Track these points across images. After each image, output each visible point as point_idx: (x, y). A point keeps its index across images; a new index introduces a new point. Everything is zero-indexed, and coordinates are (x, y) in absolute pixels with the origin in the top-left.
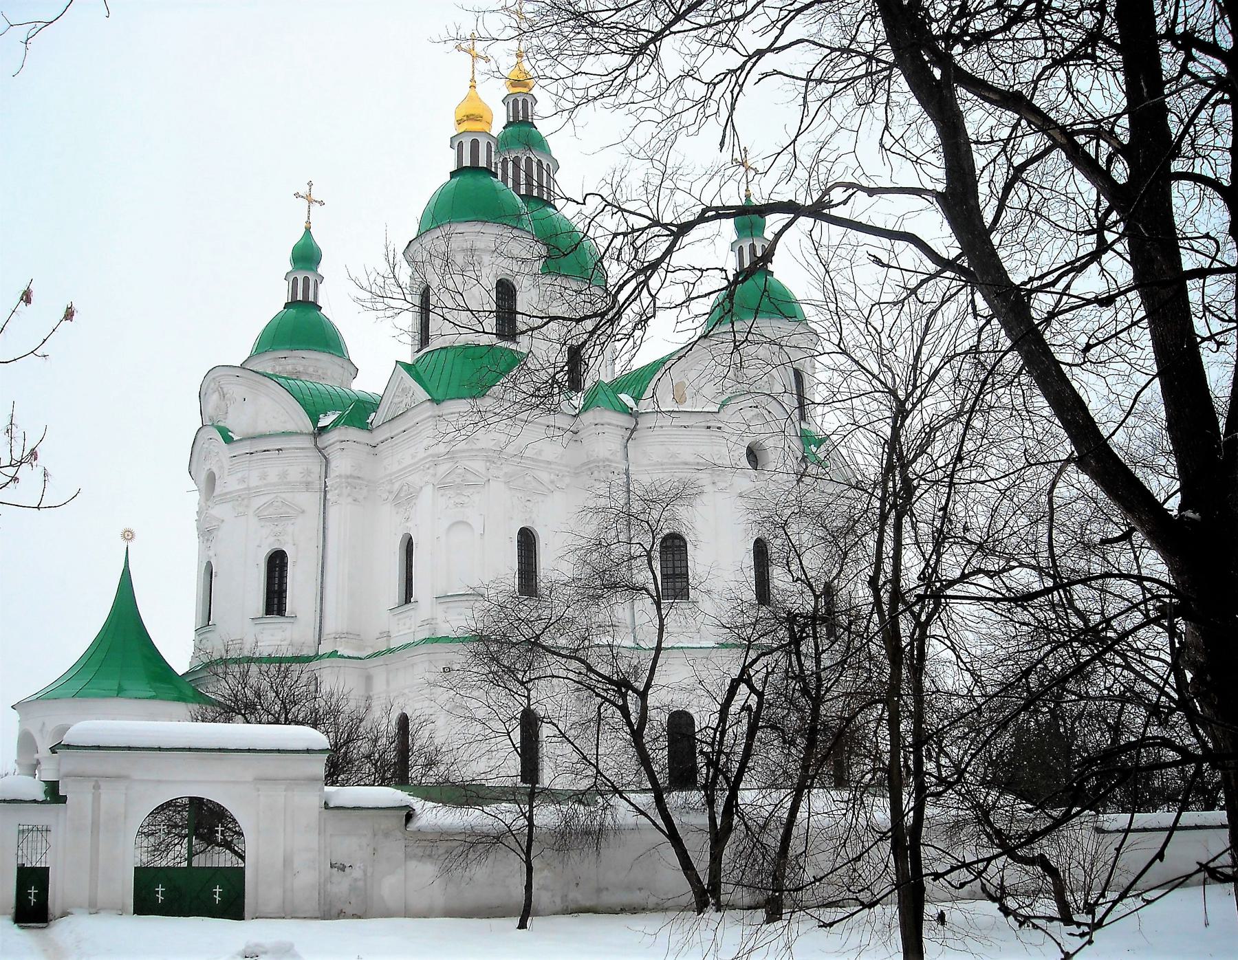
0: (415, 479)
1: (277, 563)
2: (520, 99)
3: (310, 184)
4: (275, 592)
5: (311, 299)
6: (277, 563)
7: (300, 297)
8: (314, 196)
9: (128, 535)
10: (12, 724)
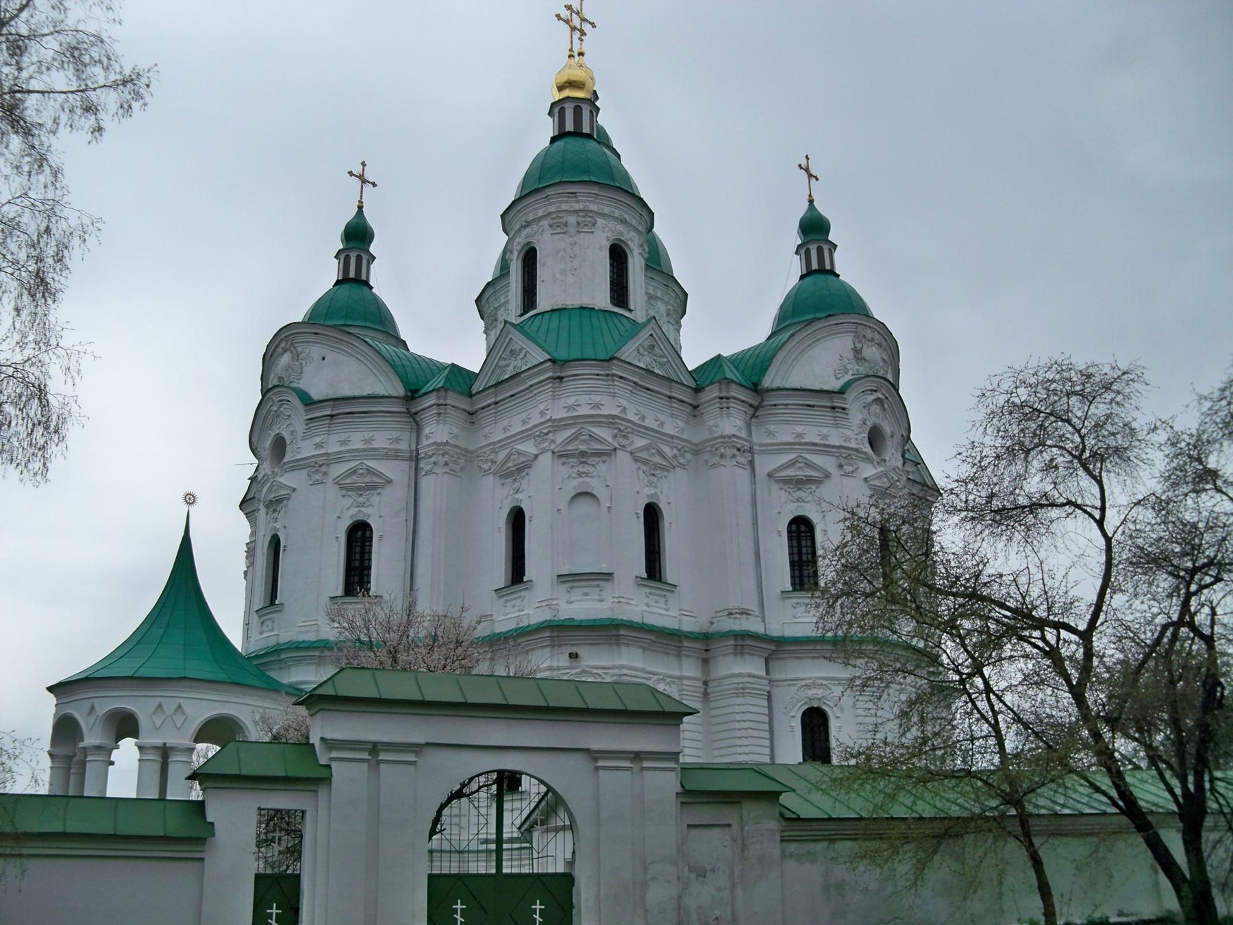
0: (529, 448)
1: (359, 537)
3: (364, 164)
4: (355, 569)
5: (364, 277)
6: (359, 537)
7: (352, 275)
8: (368, 176)
9: (190, 499)
10: (47, 709)
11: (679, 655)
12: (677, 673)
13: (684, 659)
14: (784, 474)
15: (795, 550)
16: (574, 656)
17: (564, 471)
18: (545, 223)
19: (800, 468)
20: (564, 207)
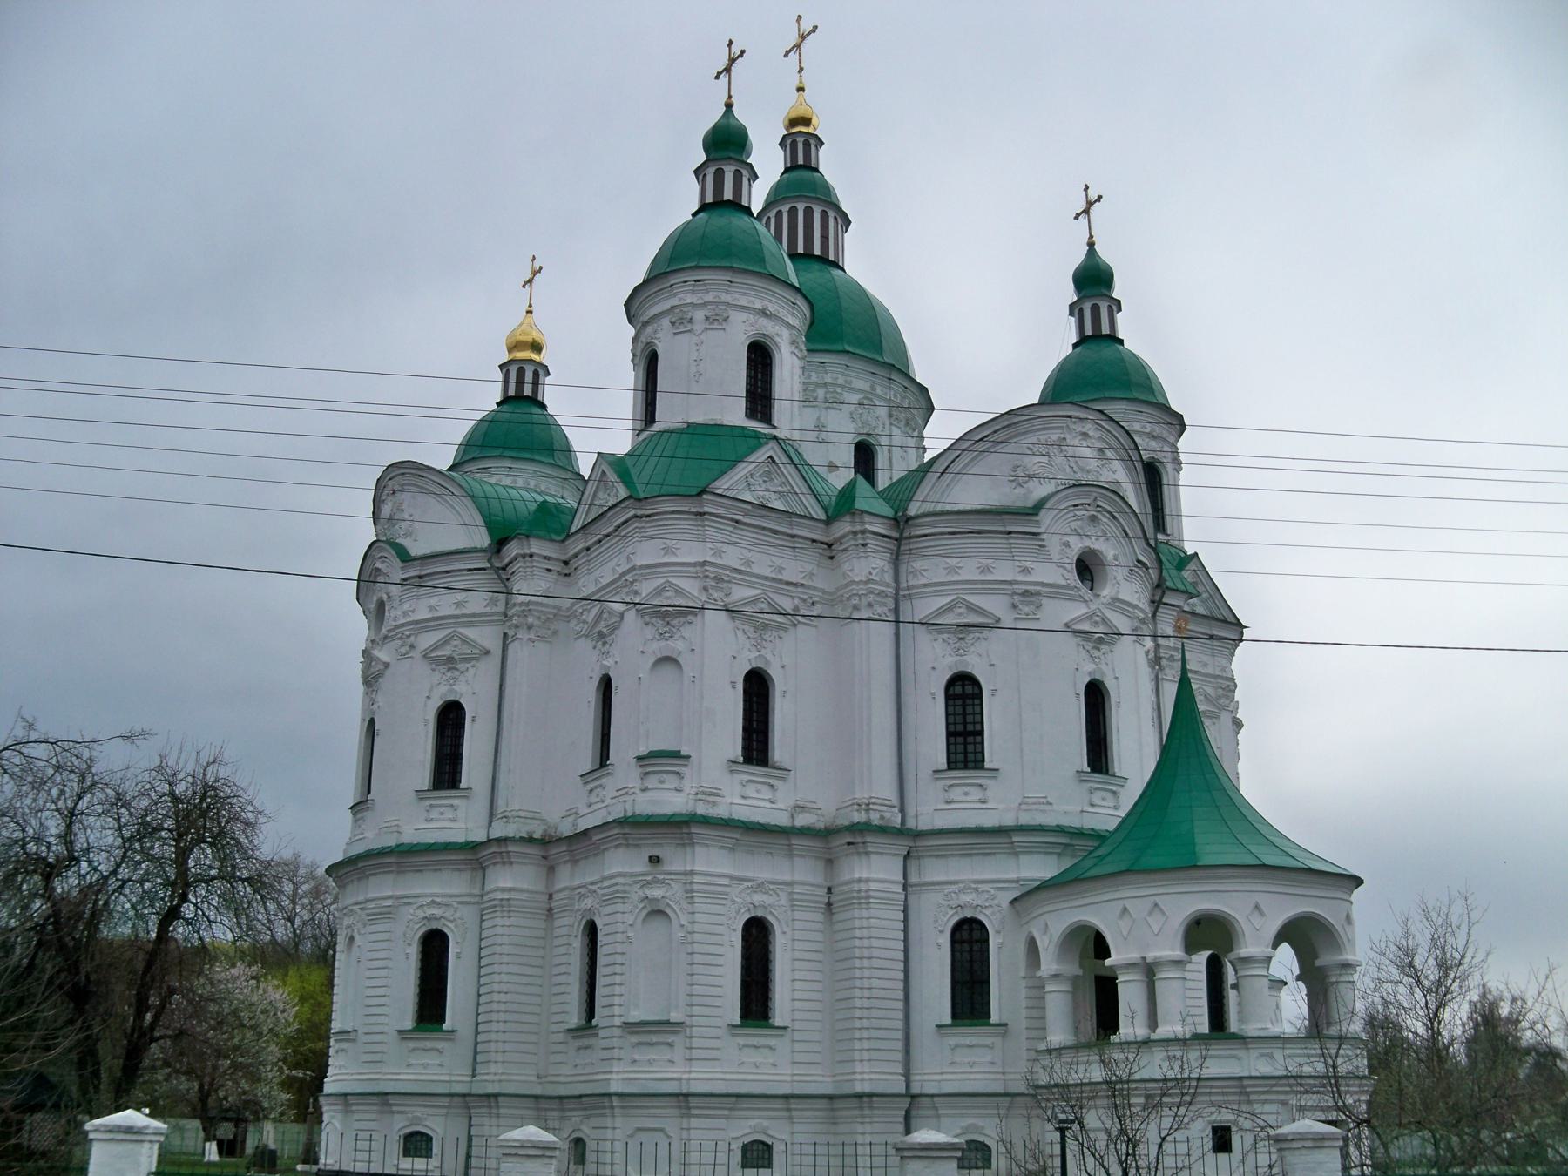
2: (800, 140)
11: (790, 854)
12: (787, 878)
13: (797, 860)
15: (959, 719)
16: (655, 860)
17: (649, 632)
18: (665, 322)
20: (689, 299)
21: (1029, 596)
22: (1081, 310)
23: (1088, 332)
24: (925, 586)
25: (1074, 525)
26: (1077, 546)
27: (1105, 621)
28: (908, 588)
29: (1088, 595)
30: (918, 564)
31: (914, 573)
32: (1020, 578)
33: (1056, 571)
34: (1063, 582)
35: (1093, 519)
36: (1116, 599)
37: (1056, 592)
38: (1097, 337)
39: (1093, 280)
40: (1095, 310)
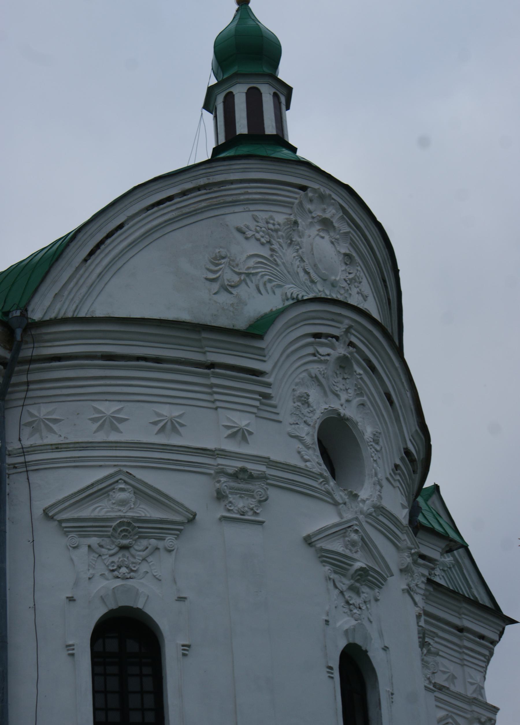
14: (86, 512)
19: (123, 503)
21: (244, 482)
22: (229, 99)
23: (242, 127)
24: (57, 447)
25: (315, 369)
26: (320, 405)
27: (366, 544)
28: (24, 452)
29: (340, 495)
30: (42, 411)
31: (35, 426)
32: (231, 446)
33: (284, 441)
34: (302, 464)
35: (344, 364)
36: (380, 509)
37: (289, 479)
38: (256, 135)
39: (247, 56)
40: (254, 99)
